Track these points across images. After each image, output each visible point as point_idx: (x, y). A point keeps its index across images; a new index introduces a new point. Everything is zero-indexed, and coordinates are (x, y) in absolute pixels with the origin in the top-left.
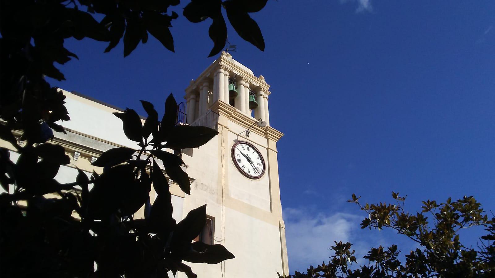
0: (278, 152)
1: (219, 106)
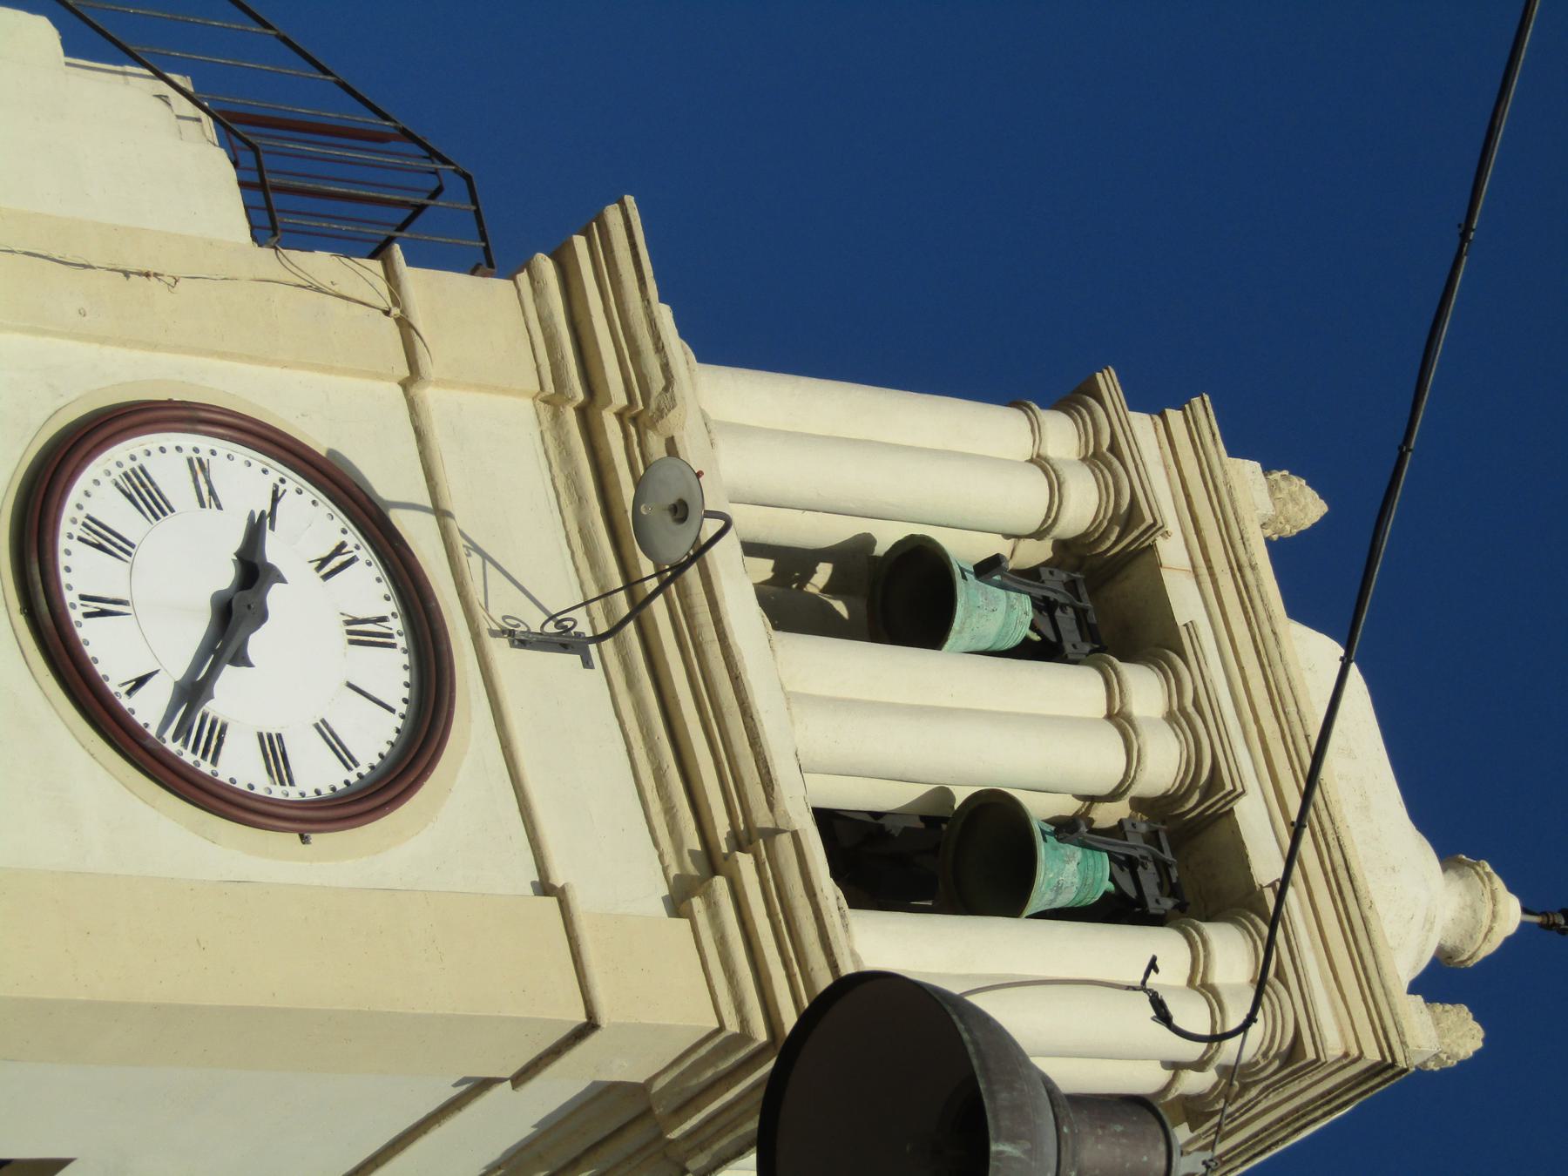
1: (580, 242)
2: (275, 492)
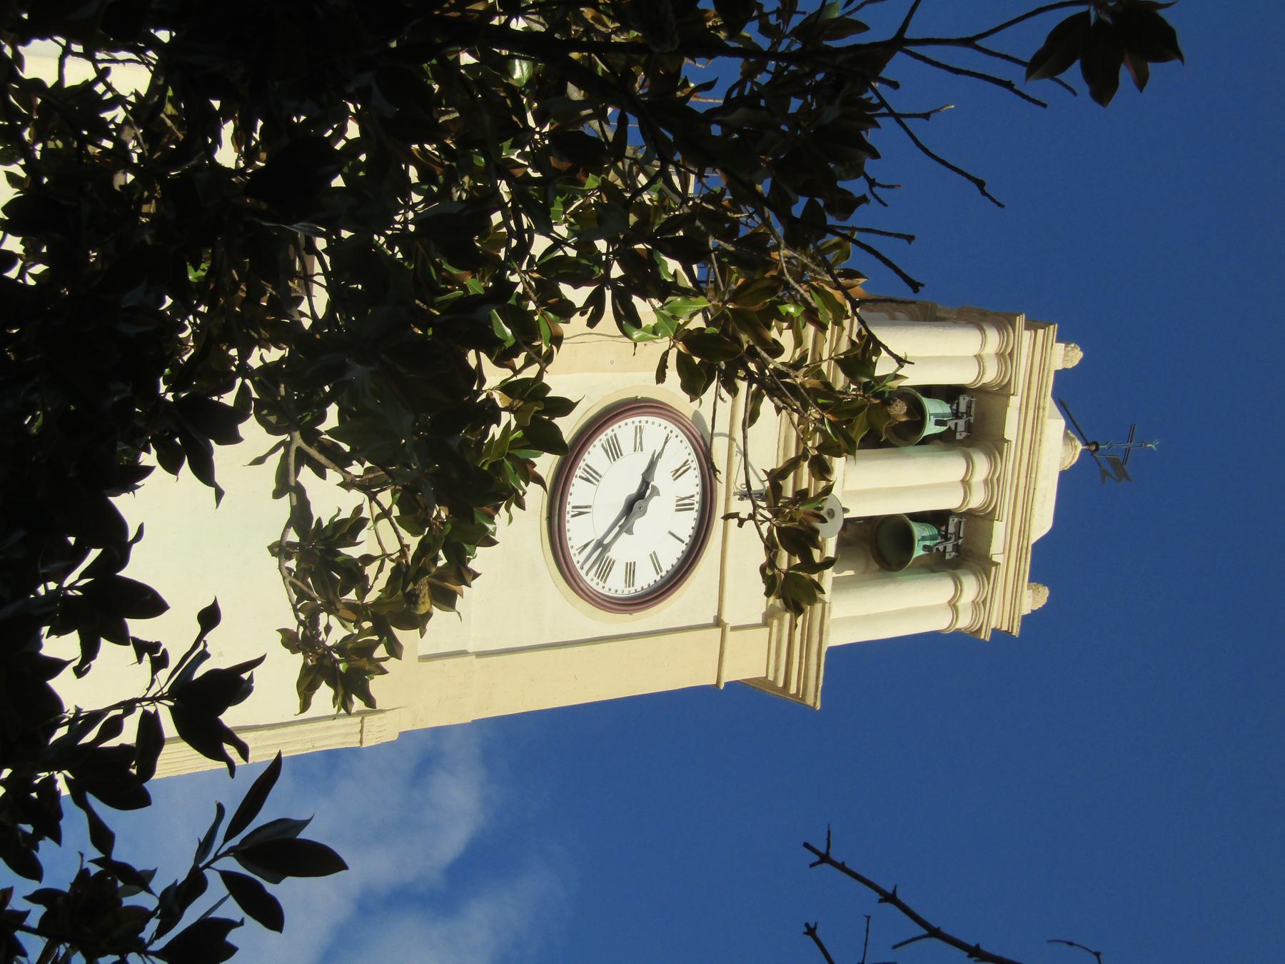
0: (722, 686)
2: (667, 438)
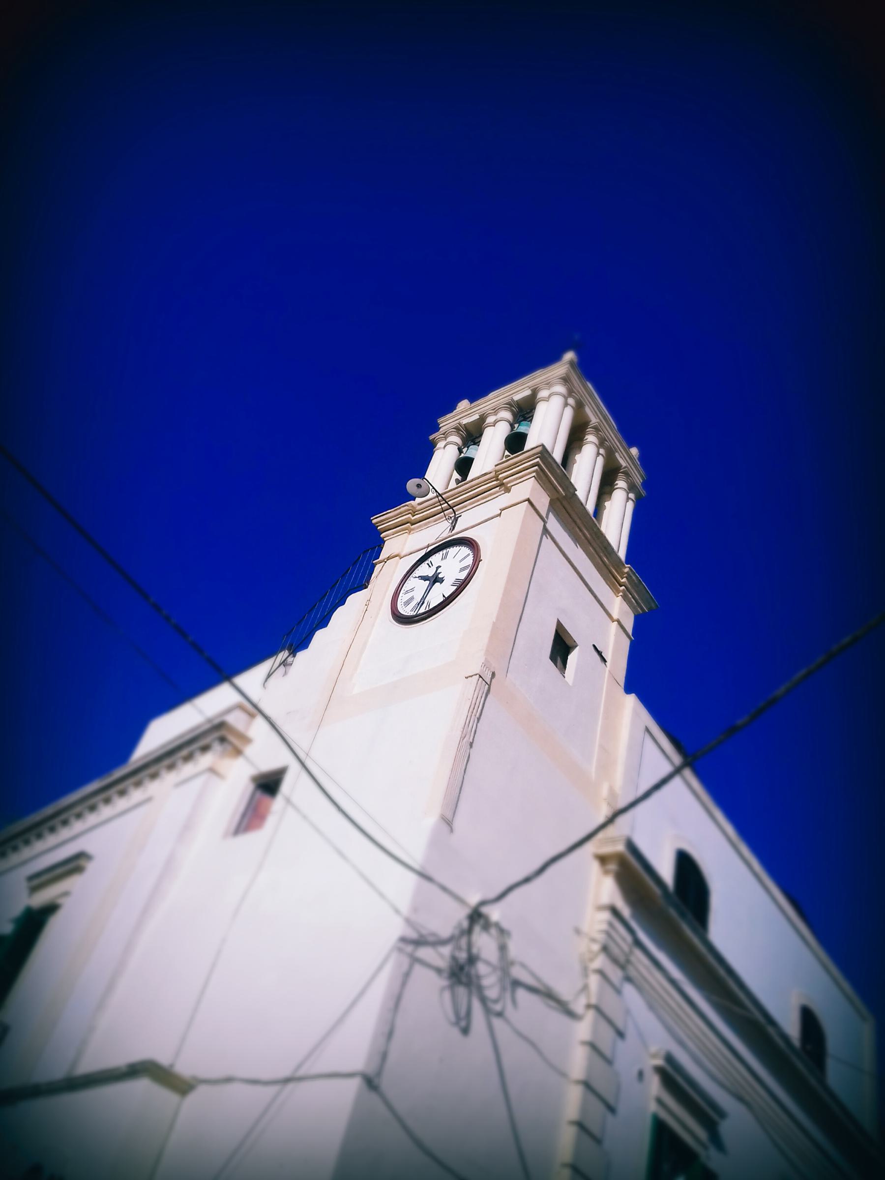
1: (379, 528)
